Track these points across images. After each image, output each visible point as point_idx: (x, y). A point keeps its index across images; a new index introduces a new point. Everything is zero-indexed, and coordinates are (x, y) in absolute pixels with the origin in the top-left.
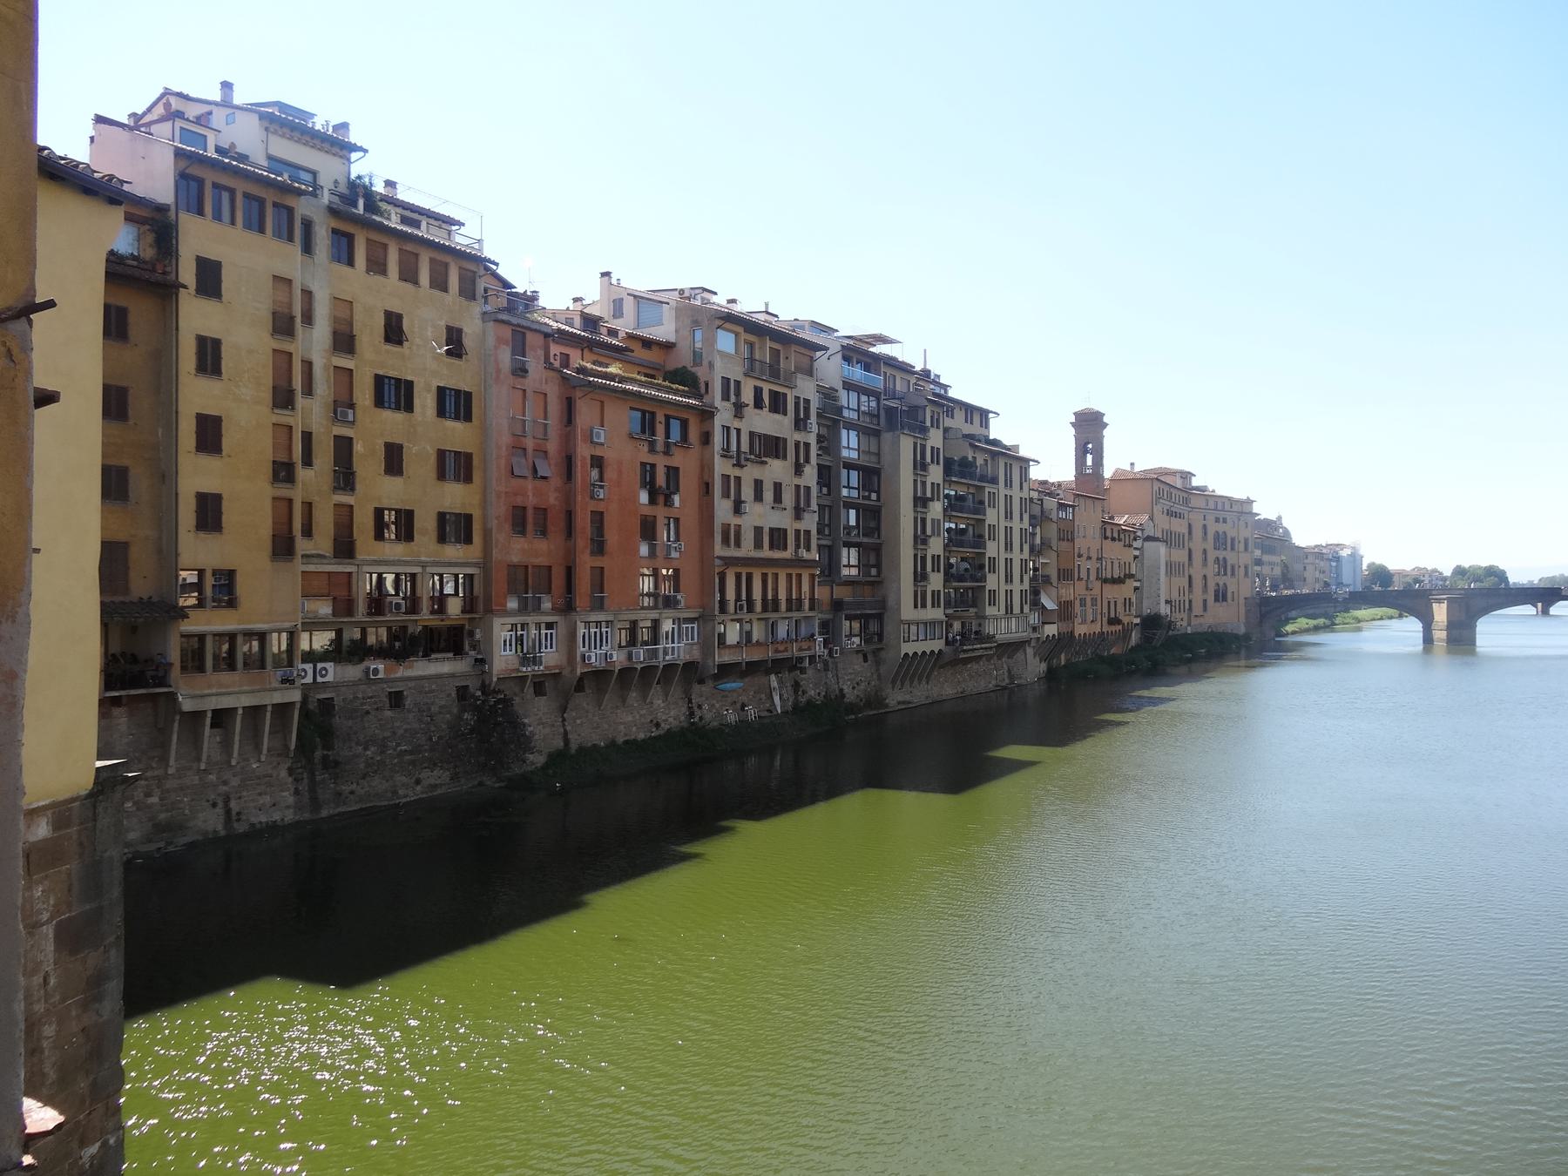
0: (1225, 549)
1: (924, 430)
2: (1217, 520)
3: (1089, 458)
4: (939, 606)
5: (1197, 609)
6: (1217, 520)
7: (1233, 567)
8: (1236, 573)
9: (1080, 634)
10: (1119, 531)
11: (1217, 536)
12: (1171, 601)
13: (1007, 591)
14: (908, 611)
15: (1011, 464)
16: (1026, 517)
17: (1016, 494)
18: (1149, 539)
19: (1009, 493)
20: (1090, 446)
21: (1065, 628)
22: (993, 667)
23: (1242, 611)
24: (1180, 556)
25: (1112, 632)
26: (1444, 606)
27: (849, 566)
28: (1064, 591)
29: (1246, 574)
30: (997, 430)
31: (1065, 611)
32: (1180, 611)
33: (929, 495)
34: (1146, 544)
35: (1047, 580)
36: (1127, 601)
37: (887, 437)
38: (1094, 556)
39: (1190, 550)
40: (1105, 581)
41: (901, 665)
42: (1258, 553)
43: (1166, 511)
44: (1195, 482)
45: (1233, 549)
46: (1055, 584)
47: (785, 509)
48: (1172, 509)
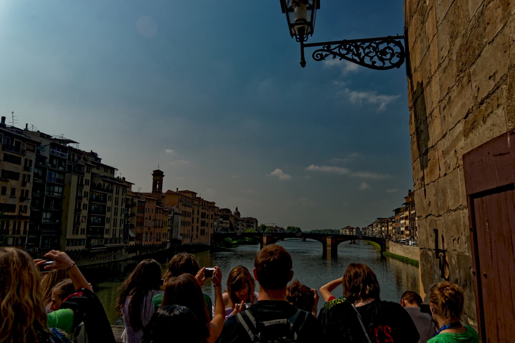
0: (205, 218)
1: (83, 174)
2: (203, 208)
4: (84, 234)
5: (194, 237)
6: (203, 208)
9: (144, 245)
11: (202, 213)
12: (184, 234)
14: (69, 235)
16: (124, 205)
17: (120, 197)
21: (138, 242)
23: (210, 238)
25: (158, 244)
26: (266, 238)
28: (139, 230)
29: (211, 226)
31: (139, 237)
32: (188, 238)
34: (175, 216)
35: (132, 226)
37: (67, 175)
38: (152, 218)
40: (156, 227)
42: (221, 219)
44: (197, 196)
45: (207, 218)
46: (135, 227)
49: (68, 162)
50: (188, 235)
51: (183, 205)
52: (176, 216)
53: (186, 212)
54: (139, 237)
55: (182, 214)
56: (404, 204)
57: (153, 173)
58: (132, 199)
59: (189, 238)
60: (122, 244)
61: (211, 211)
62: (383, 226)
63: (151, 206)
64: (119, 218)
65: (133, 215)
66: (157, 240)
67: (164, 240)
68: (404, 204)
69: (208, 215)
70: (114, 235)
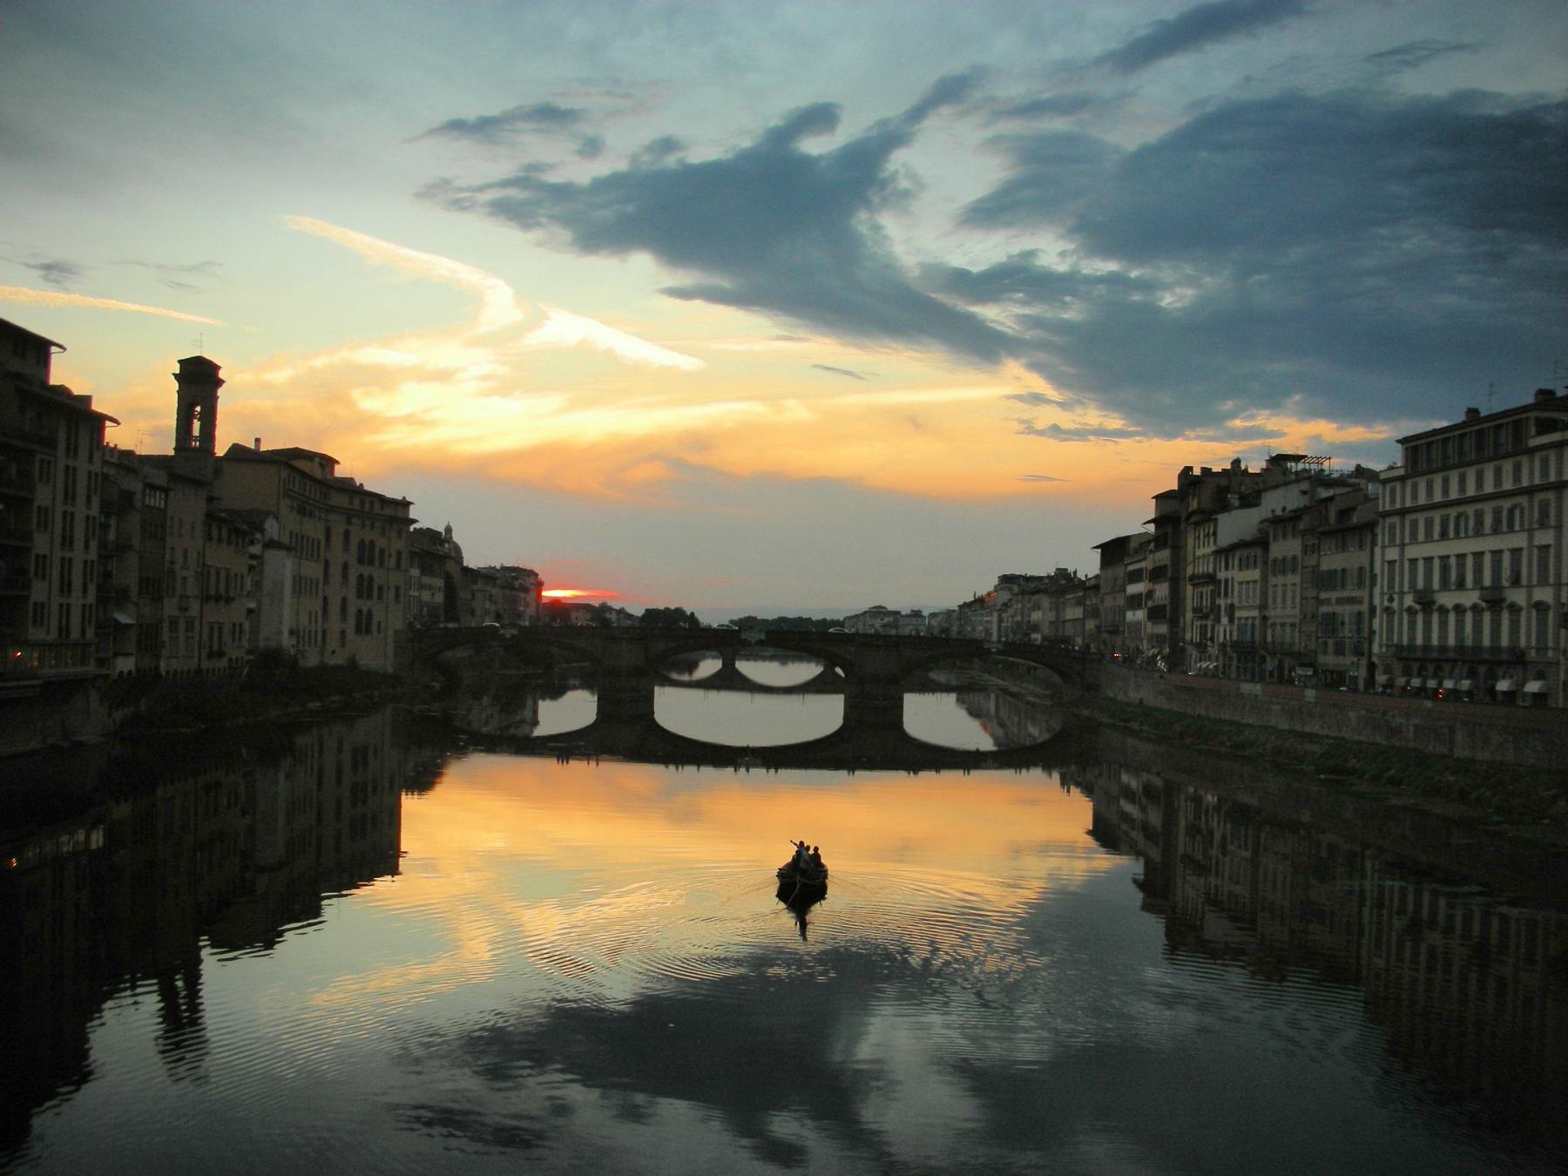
0: (371, 563)
2: (363, 526)
3: (197, 425)
5: (333, 643)
7: (380, 588)
9: (167, 673)
10: (229, 530)
12: (298, 630)
16: (95, 500)
17: (82, 466)
18: (271, 545)
20: (198, 409)
24: (313, 570)
29: (397, 596)
30: (61, 372)
36: (237, 629)
40: (205, 598)
43: (296, 507)
44: (340, 472)
45: (382, 564)
50: (310, 632)
53: (302, 537)
54: (149, 639)
56: (1149, 522)
57: (178, 372)
60: (91, 668)
61: (394, 534)
62: (1038, 607)
63: (188, 508)
64: (78, 556)
65: (123, 547)
66: (211, 655)
67: (235, 654)
68: (1149, 522)
69: (382, 551)
70: (64, 630)
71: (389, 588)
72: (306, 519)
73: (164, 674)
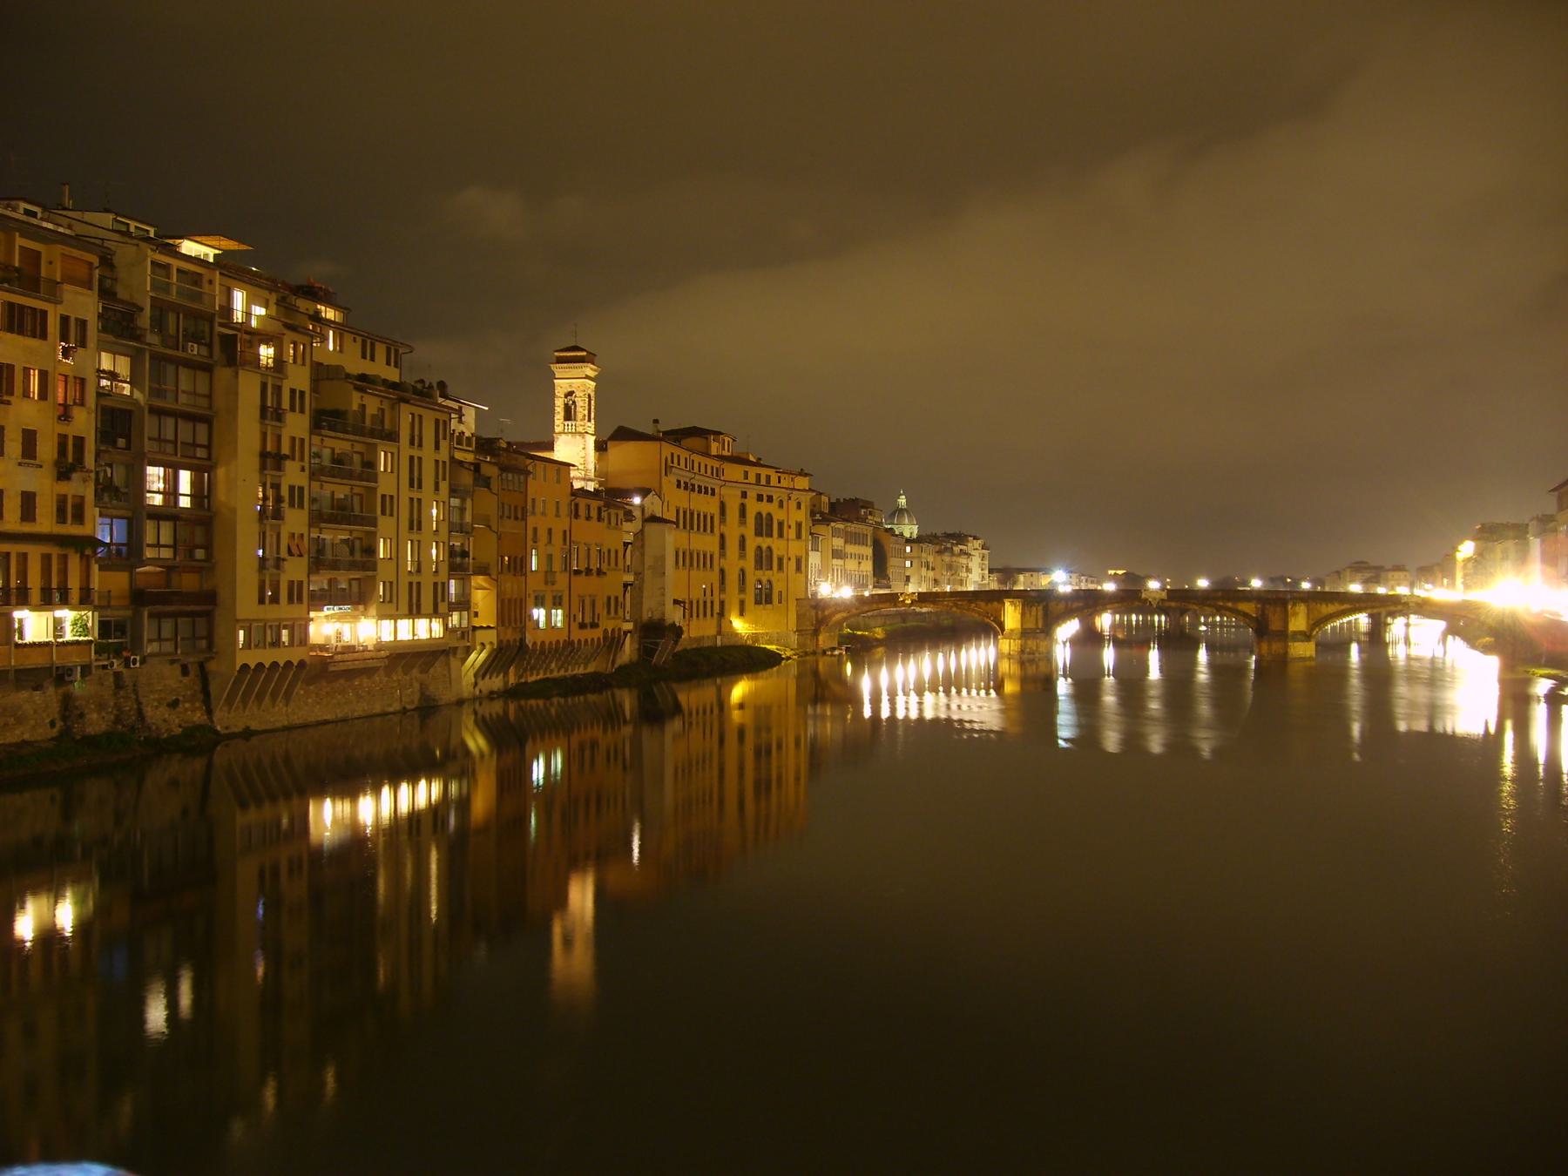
2: (760, 498)
6: (760, 498)
7: (780, 560)
8: (785, 565)
9: (535, 643)
12: (691, 603)
13: (411, 584)
15: (420, 416)
17: (428, 454)
19: (416, 453)
22: (396, 684)
24: (707, 543)
25: (586, 641)
27: (158, 545)
32: (705, 615)
33: (285, 450)
39: (722, 537)
41: (238, 682)
42: (838, 542)
45: (781, 535)
47: (41, 467)
48: (693, 481)
49: (221, 325)
50: (705, 602)
51: (679, 486)
52: (652, 528)
53: (692, 514)
55: (678, 527)
58: (477, 467)
59: (712, 615)
66: (582, 626)
67: (608, 624)
69: (781, 524)
71: (789, 559)
72: (694, 495)
73: (530, 646)
